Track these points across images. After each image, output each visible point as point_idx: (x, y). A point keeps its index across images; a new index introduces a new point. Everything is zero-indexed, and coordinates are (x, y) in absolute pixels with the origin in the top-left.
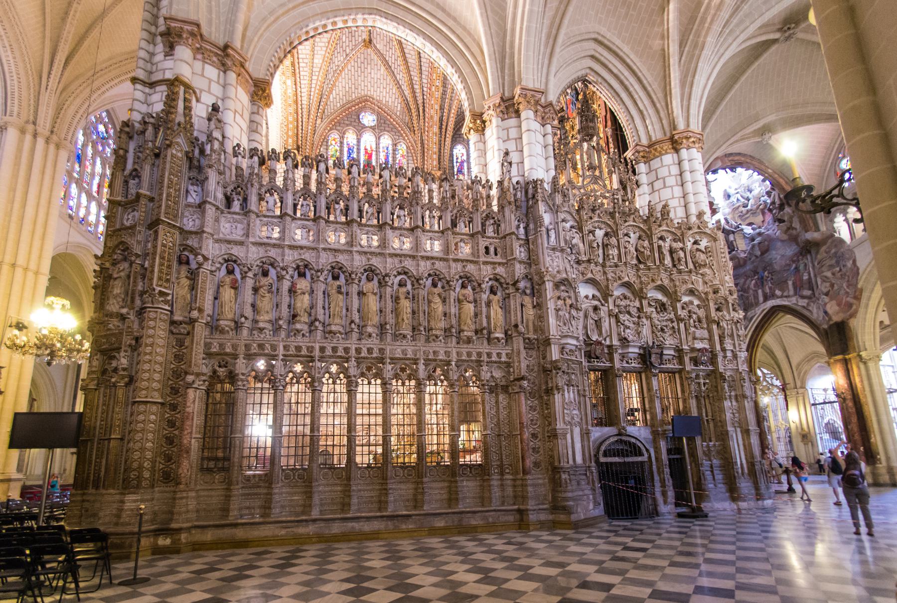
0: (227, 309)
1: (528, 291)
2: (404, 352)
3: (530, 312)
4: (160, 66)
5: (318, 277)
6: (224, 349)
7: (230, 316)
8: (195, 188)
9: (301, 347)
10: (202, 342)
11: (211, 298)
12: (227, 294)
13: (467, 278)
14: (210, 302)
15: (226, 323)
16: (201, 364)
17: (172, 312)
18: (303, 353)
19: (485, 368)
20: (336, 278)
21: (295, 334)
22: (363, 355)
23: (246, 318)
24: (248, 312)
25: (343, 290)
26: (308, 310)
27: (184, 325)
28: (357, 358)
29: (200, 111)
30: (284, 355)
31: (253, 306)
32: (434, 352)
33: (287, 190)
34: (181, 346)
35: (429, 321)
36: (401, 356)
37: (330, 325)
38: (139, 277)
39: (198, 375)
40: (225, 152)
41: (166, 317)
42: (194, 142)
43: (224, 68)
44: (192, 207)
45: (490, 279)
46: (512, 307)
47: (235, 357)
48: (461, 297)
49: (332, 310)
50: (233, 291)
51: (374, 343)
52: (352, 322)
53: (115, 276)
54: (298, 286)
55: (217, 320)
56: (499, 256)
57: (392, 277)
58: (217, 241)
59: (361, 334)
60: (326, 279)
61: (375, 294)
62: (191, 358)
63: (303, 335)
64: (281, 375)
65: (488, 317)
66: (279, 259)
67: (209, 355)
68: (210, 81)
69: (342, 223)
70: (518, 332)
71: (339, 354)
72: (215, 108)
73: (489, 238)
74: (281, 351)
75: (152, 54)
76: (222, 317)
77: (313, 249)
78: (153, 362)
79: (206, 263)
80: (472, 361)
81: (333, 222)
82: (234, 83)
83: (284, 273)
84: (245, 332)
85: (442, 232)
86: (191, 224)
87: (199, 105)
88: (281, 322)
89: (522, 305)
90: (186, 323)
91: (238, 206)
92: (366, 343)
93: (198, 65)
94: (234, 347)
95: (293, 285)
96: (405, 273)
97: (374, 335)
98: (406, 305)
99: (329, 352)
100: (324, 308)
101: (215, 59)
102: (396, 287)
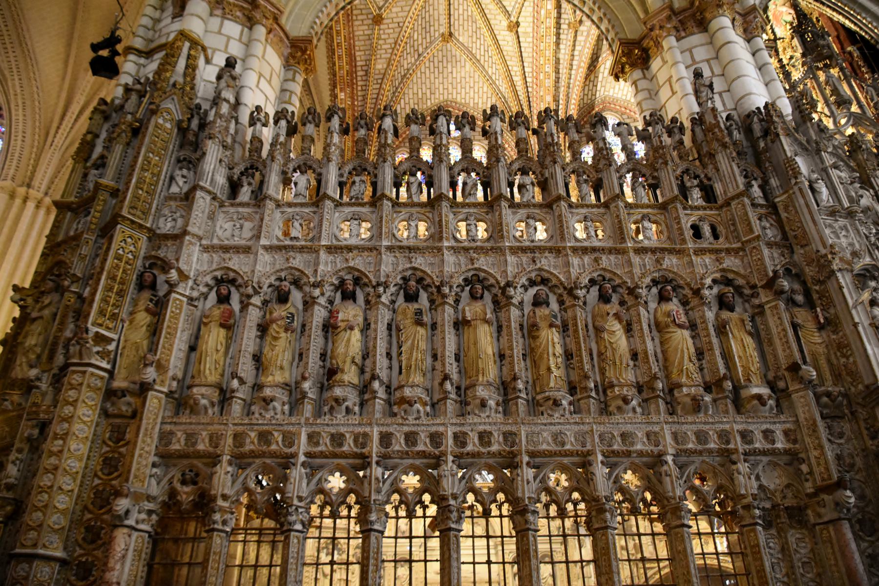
1: (800, 298)
2: (558, 438)
3: (814, 339)
4: (165, 31)
5: (379, 296)
6: (194, 444)
7: (212, 377)
8: (185, 172)
9: (342, 435)
11: (185, 347)
12: (214, 337)
13: (667, 281)
14: (182, 355)
15: (203, 390)
16: (146, 477)
17: (111, 373)
18: (345, 448)
19: (743, 467)
20: (412, 297)
21: (332, 408)
22: (470, 448)
23: (242, 381)
24: (246, 368)
25: (426, 319)
26: (358, 359)
28: (458, 457)
29: (207, 73)
30: (308, 455)
31: (257, 358)
32: (623, 436)
33: (329, 160)
35: (602, 372)
36: (553, 448)
37: (401, 387)
38: (71, 314)
39: (137, 497)
40: (237, 122)
41: (99, 383)
42: (195, 110)
43: (250, 22)
44: (175, 199)
45: (714, 281)
46: (774, 331)
47: (214, 460)
48: (661, 318)
49: (404, 357)
50: (223, 332)
51: (491, 420)
52: (446, 377)
53: (34, 315)
54: (341, 316)
55: (190, 387)
56: (721, 240)
57: (520, 290)
58: (206, 249)
59: (463, 403)
60: (393, 302)
61: (487, 321)
62: (131, 463)
63: (348, 410)
64: (300, 499)
65: (727, 356)
66: (309, 271)
67: (166, 457)
68: (229, 38)
69: (421, 205)
70: (801, 380)
71: (420, 447)
72: (230, 63)
73: (697, 208)
74: (303, 445)
75: (157, 21)
76: (197, 381)
77: (370, 249)
78: (60, 471)
79: (182, 285)
80: (710, 451)
81: (405, 205)
82: (263, 39)
83: (317, 292)
84: (237, 408)
85: (606, 205)
86: (169, 225)
87: (209, 68)
88: (306, 385)
89: (795, 326)
90: (132, 393)
92: (478, 422)
93: (215, 22)
94: (215, 439)
95: (332, 314)
96: (544, 281)
97: (492, 403)
98: (552, 340)
99: (399, 444)
100: (389, 355)
101: (238, 14)
102: (527, 309)
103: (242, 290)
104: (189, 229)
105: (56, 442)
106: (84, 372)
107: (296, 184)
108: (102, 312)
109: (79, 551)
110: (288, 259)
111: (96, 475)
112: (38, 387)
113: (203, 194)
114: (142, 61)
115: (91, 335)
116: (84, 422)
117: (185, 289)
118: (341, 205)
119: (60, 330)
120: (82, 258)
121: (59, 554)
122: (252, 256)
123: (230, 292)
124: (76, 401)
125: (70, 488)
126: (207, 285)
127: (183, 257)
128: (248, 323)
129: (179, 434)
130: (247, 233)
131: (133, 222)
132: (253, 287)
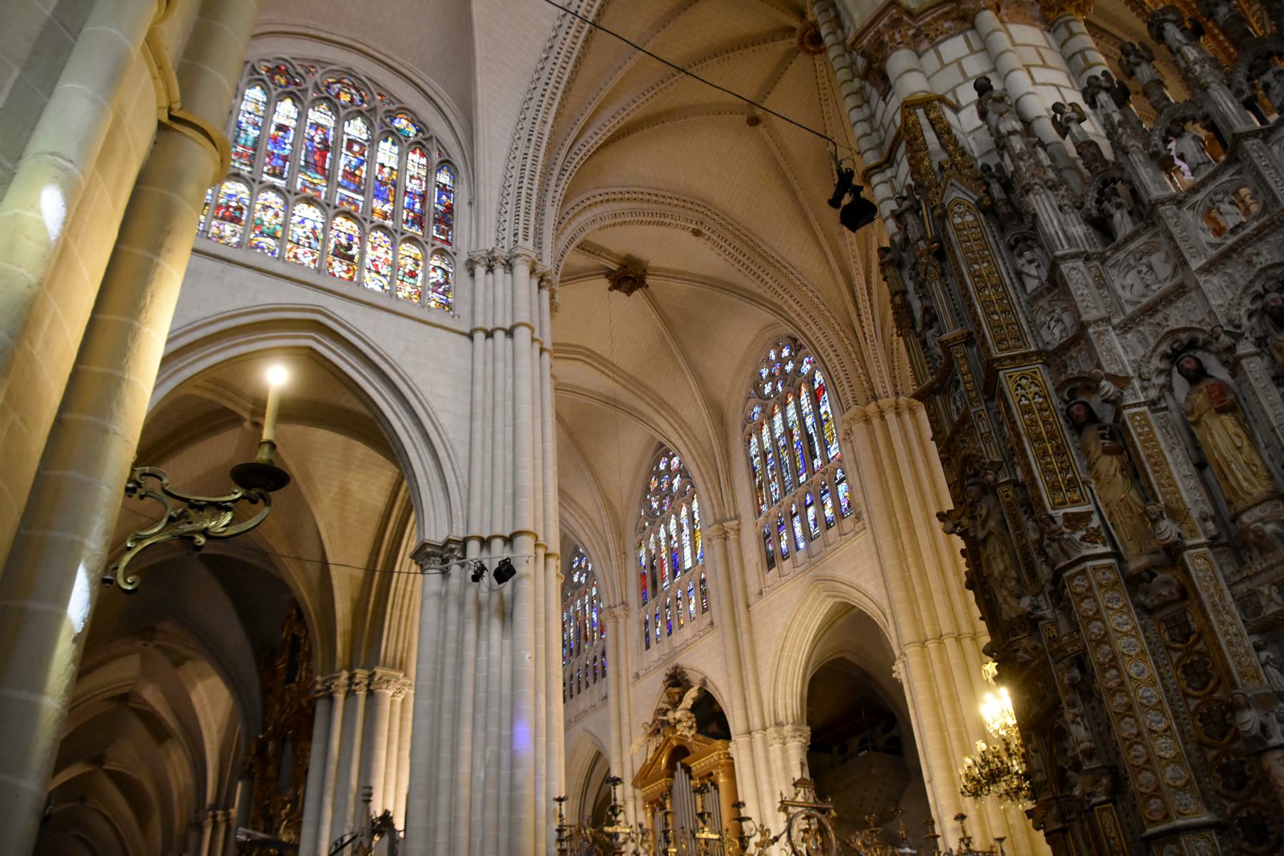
0: (1240, 474)
4: (886, 121)
8: (1028, 255)
10: (1229, 598)
11: (1188, 469)
12: (1222, 434)
15: (1257, 512)
17: (1116, 554)
27: (1161, 576)
29: (966, 122)
33: (1204, 88)
34: (1186, 637)
38: (1021, 511)
40: (1044, 147)
41: (1111, 576)
42: (985, 176)
43: (967, 21)
50: (1228, 420)
53: (981, 535)
55: (1235, 518)
58: (1125, 328)
62: (1223, 658)
68: (958, 62)
72: (983, 87)
75: (870, 118)
76: (1240, 505)
78: (1137, 708)
82: (997, 24)
86: (1056, 331)
87: (962, 114)
90: (1162, 567)
91: (1127, 219)
93: (930, 59)
101: (946, 25)
103: (1213, 347)
104: (1085, 318)
105: (1108, 675)
106: (1084, 572)
107: (1181, 157)
108: (1054, 488)
109: (1230, 807)
110: (1249, 262)
111: (1186, 695)
112: (1042, 618)
113: (1070, 264)
114: (889, 173)
115: (1060, 522)
116: (1126, 634)
117: (1135, 395)
118: (1272, 130)
119: (1021, 536)
120: (987, 439)
121: (1205, 818)
122: (1193, 294)
123: (1198, 361)
124: (1098, 611)
125: (1163, 726)
126: (1160, 372)
127: (1104, 359)
128: (1257, 386)
129: (1265, 590)
130: (1164, 270)
131: (1013, 358)
132: (1227, 333)
